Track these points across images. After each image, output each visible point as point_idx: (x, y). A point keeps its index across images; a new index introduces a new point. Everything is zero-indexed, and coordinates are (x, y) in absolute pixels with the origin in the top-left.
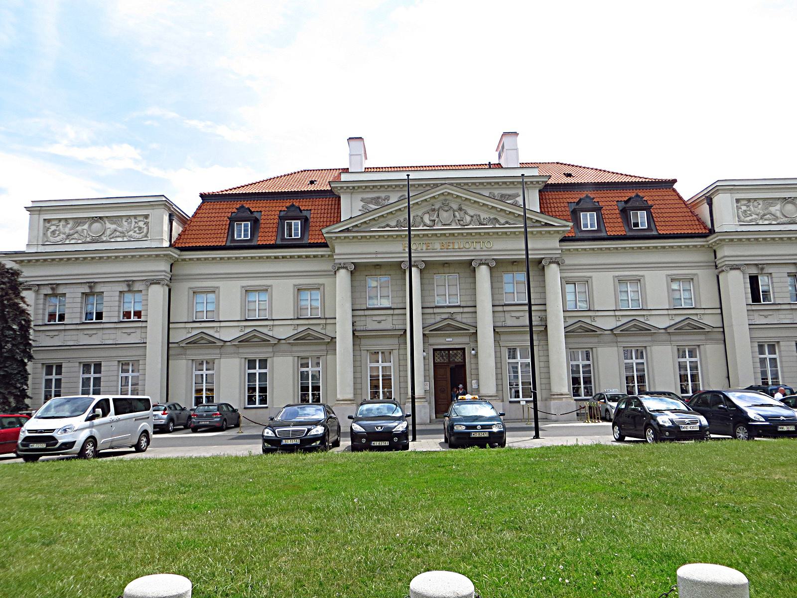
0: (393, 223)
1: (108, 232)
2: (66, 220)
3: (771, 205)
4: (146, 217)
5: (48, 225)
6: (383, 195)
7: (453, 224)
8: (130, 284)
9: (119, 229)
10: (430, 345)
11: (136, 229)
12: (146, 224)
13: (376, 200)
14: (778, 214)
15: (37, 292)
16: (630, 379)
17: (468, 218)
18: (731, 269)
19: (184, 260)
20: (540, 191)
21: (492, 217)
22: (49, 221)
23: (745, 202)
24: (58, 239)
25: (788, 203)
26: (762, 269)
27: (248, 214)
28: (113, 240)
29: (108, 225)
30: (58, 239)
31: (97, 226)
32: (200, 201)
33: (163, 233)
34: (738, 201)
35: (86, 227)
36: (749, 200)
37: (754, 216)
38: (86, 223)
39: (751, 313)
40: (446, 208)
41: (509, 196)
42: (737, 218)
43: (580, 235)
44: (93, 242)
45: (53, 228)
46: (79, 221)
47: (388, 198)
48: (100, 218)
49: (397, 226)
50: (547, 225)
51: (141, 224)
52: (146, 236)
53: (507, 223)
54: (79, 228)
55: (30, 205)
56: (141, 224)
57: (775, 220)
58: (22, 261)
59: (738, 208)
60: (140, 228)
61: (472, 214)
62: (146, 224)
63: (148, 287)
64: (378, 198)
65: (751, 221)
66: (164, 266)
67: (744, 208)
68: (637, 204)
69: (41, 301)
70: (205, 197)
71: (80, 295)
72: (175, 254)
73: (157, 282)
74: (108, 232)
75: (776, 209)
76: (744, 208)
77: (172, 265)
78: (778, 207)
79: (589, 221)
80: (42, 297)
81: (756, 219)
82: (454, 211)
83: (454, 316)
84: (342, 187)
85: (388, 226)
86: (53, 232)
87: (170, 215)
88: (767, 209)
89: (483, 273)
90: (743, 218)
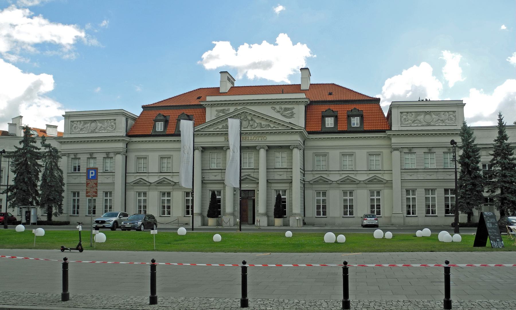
0: (220, 127)
1: (98, 128)
2: (80, 121)
3: (418, 115)
4: (115, 120)
5: (72, 124)
6: (226, 108)
7: (249, 127)
8: (108, 153)
9: (103, 126)
12: (115, 123)
13: (223, 111)
14: (422, 120)
15: (68, 157)
16: (372, 207)
17: (256, 125)
19: (132, 141)
20: (305, 107)
21: (267, 124)
22: (73, 121)
23: (406, 114)
24: (77, 130)
25: (428, 114)
26: (410, 150)
27: (162, 118)
29: (98, 124)
30: (77, 130)
31: (93, 125)
34: (401, 113)
35: (89, 125)
36: (407, 112)
37: (410, 121)
40: (245, 119)
42: (400, 123)
44: (92, 132)
45: (75, 125)
46: (85, 122)
47: (229, 110)
50: (292, 129)
51: (113, 124)
53: (274, 127)
54: (86, 126)
55: (64, 114)
56: (113, 124)
57: (420, 123)
58: (62, 142)
59: (401, 117)
60: (112, 126)
61: (258, 122)
62: (115, 123)
63: (115, 155)
64: (224, 110)
65: (407, 124)
67: (404, 117)
68: (355, 113)
71: (86, 159)
72: (128, 139)
73: (119, 153)
74: (98, 128)
75: (421, 117)
76: (404, 117)
77: (127, 144)
78: (422, 116)
79: (330, 122)
81: (410, 123)
82: (249, 121)
85: (218, 128)
86: (75, 127)
87: (127, 119)
88: (416, 117)
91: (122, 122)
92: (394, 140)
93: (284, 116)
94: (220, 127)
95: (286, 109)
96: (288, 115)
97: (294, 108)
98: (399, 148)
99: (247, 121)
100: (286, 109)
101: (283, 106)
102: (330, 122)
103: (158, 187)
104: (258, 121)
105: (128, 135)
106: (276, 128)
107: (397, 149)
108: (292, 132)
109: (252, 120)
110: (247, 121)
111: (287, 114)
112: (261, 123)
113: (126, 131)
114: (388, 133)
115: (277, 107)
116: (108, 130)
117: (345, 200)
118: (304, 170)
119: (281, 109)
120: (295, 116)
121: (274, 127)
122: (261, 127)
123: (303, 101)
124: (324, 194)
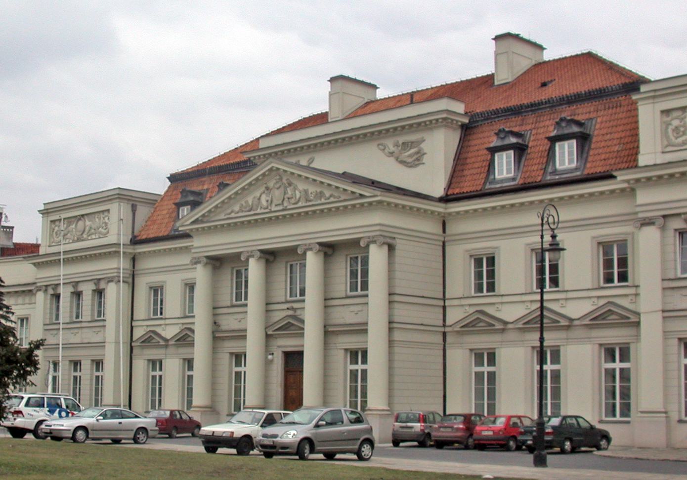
0: (237, 208)
5: (53, 226)
10: (279, 347)
11: (104, 225)
18: (643, 225)
21: (318, 191)
28: (89, 238)
29: (88, 223)
32: (169, 183)
33: (116, 228)
35: (74, 226)
38: (74, 221)
39: (668, 292)
41: (412, 142)
43: (549, 178)
44: (79, 240)
46: (69, 220)
48: (83, 216)
49: (241, 211)
52: (108, 232)
55: (42, 208)
58: (39, 263)
66: (121, 264)
69: (49, 302)
70: (173, 178)
72: (130, 250)
80: (49, 297)
83: (298, 312)
84: (254, 157)
85: (232, 212)
89: (313, 262)
90: (673, 139)
91: (118, 211)
92: (644, 197)
93: (402, 162)
94: (237, 208)
95: (406, 146)
96: (410, 160)
97: (423, 141)
98: (656, 217)
99: (282, 189)
100: (406, 146)
101: (401, 139)
102: (505, 167)
103: (596, 333)
104: (301, 186)
105: (135, 241)
106: (335, 197)
107: (648, 222)
108: (362, 205)
109: (290, 184)
110: (282, 189)
111: (410, 156)
112: (306, 191)
113: (133, 232)
114: (623, 178)
115: (390, 143)
116: (100, 233)
117: (611, 374)
118: (444, 299)
119: (398, 146)
120: (425, 159)
121: (331, 196)
122: (307, 200)
123: (437, 120)
124: (492, 360)
